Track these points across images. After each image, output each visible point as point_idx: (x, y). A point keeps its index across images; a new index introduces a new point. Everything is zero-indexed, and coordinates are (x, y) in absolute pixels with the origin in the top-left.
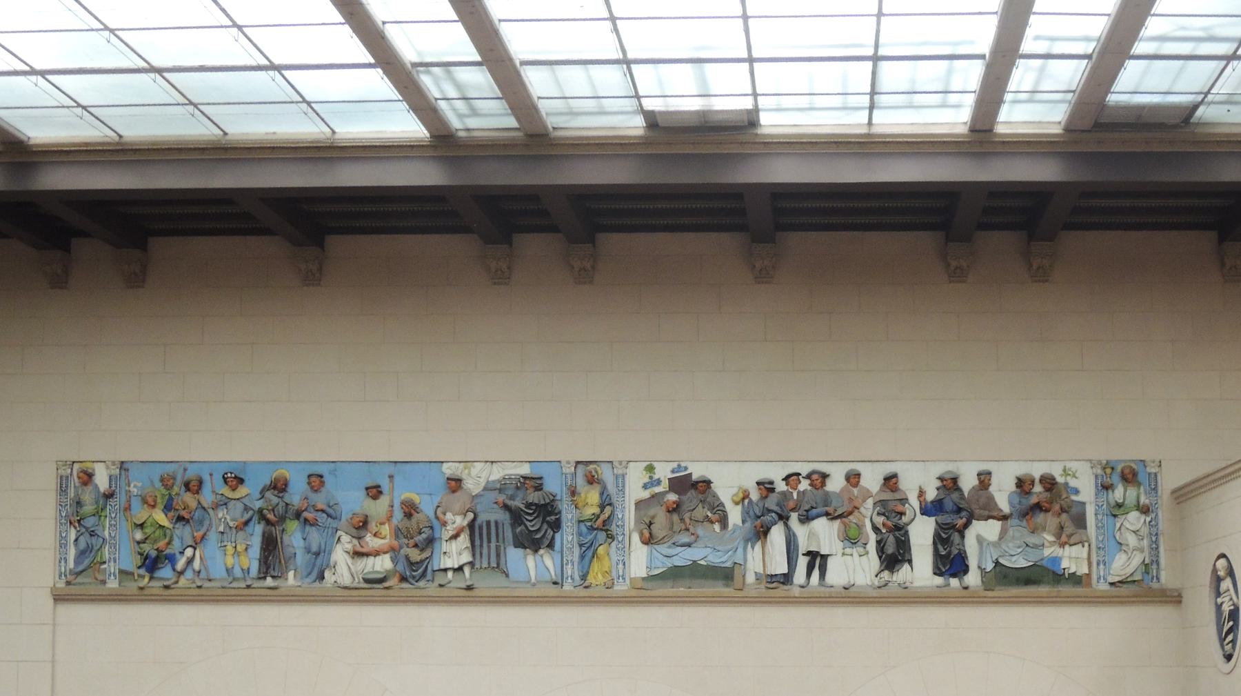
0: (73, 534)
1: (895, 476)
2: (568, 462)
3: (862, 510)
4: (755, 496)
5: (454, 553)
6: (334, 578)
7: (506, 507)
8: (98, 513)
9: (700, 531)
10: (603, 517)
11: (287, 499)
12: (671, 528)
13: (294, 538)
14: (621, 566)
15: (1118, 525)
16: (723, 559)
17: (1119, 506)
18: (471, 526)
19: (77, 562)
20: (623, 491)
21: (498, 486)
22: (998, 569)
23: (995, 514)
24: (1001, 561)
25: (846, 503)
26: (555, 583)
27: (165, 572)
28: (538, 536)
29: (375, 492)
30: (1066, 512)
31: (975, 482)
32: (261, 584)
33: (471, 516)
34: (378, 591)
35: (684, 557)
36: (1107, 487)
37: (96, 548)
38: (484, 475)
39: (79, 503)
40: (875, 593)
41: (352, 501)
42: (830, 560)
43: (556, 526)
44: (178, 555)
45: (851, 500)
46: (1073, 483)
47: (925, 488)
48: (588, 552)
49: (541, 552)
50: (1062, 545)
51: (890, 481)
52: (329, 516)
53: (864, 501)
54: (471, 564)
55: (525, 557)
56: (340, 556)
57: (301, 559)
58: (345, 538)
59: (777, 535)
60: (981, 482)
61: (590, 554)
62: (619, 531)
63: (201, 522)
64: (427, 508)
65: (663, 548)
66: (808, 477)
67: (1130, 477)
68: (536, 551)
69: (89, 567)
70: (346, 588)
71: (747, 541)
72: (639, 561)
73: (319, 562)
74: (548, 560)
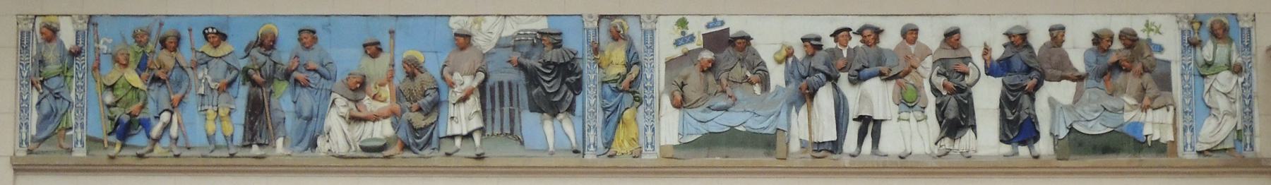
0: (35, 97)
1: (956, 31)
2: (591, 16)
3: (920, 69)
4: (800, 54)
5: (462, 118)
6: (327, 146)
7: (521, 66)
8: (63, 73)
9: (738, 93)
10: (629, 78)
11: (275, 57)
12: (706, 90)
13: (283, 100)
14: (649, 132)
15: (1207, 87)
16: (765, 125)
17: (1208, 65)
18: (482, 87)
19: (40, 127)
20: (652, 48)
21: (512, 43)
22: (1072, 136)
23: (1069, 74)
24: (1076, 127)
25: (902, 62)
26: (576, 152)
27: (139, 139)
28: (557, 99)
29: (373, 49)
30: (1149, 72)
31: (1047, 38)
32: (245, 152)
33: (481, 76)
34: (377, 161)
35: (720, 122)
36: (1195, 44)
37: (61, 113)
38: (496, 30)
39: (42, 62)
40: (934, 163)
41: (346, 58)
42: (884, 127)
43: (577, 87)
44: (153, 121)
45: (907, 58)
46: (1156, 39)
47: (991, 45)
48: (613, 117)
49: (561, 116)
50: (1145, 109)
51: (952, 37)
52: (322, 76)
53: (922, 60)
54: (482, 130)
55: (542, 123)
56: (334, 121)
57: (291, 124)
58: (341, 101)
59: (825, 97)
60: (1054, 38)
61: (615, 118)
62: (648, 93)
63: (179, 84)
64: (432, 67)
65: (698, 113)
66: (860, 32)
67: (1220, 32)
68: (554, 116)
69: (54, 133)
70: (341, 157)
71: (791, 104)
72: (670, 126)
73: (311, 128)
74: (568, 127)
